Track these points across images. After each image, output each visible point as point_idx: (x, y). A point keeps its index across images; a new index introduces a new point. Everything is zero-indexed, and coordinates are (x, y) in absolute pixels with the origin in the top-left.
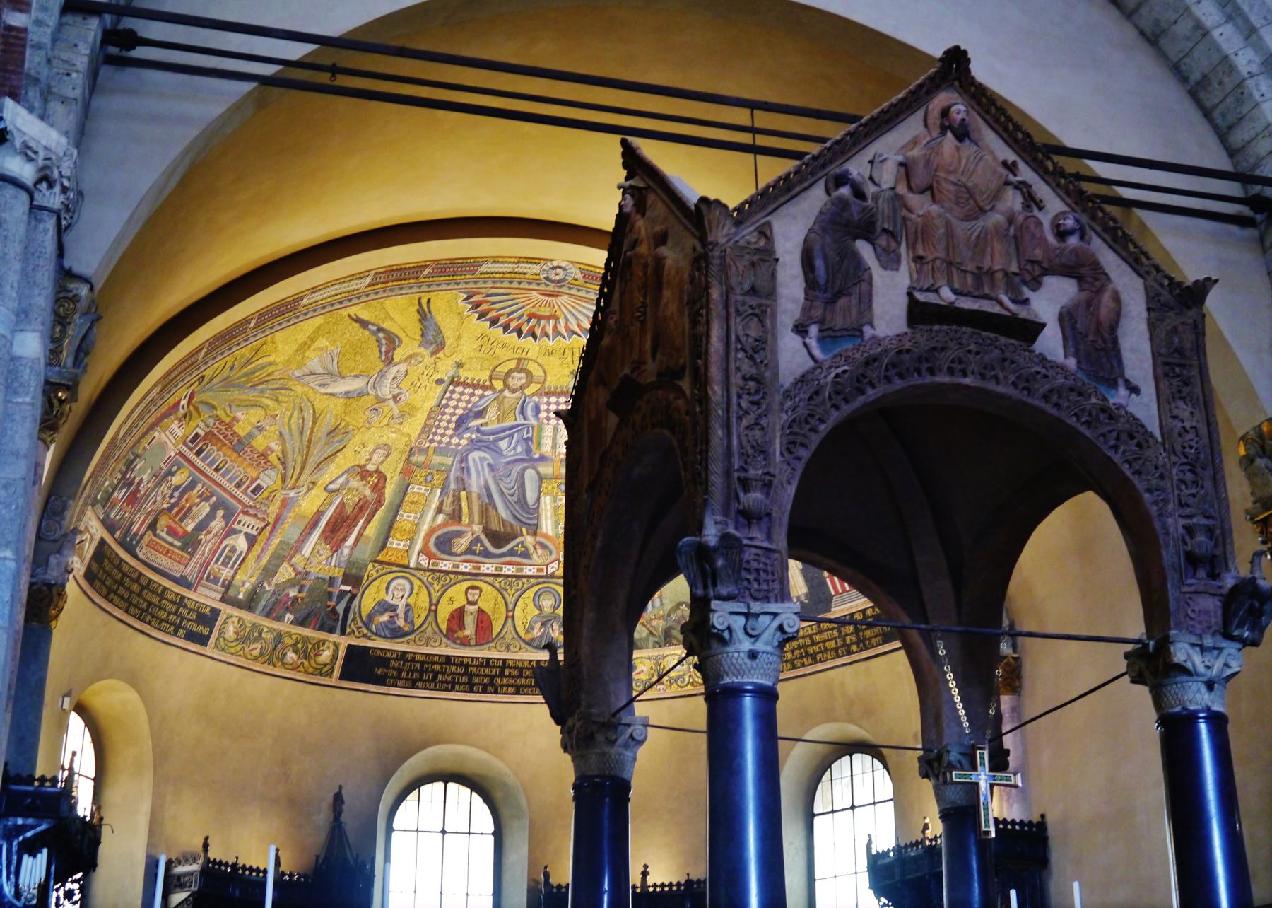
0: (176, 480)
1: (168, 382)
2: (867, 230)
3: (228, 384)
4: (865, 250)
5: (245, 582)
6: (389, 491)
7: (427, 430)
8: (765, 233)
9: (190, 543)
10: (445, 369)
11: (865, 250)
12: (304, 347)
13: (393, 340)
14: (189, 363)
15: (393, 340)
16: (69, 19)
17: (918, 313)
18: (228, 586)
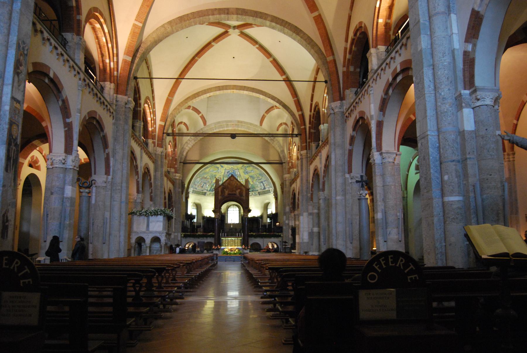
0: (200, 182)
1: (196, 176)
2: (225, 188)
3: (203, 174)
4: (225, 190)
5: (209, 189)
6: (222, 179)
7: (224, 173)
8: (218, 190)
9: (202, 187)
10: (224, 169)
11: (225, 190)
12: (210, 170)
13: (218, 168)
14: (198, 174)
15: (218, 168)
16: (181, 163)
17: (228, 194)
18: (207, 190)
